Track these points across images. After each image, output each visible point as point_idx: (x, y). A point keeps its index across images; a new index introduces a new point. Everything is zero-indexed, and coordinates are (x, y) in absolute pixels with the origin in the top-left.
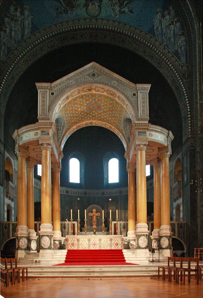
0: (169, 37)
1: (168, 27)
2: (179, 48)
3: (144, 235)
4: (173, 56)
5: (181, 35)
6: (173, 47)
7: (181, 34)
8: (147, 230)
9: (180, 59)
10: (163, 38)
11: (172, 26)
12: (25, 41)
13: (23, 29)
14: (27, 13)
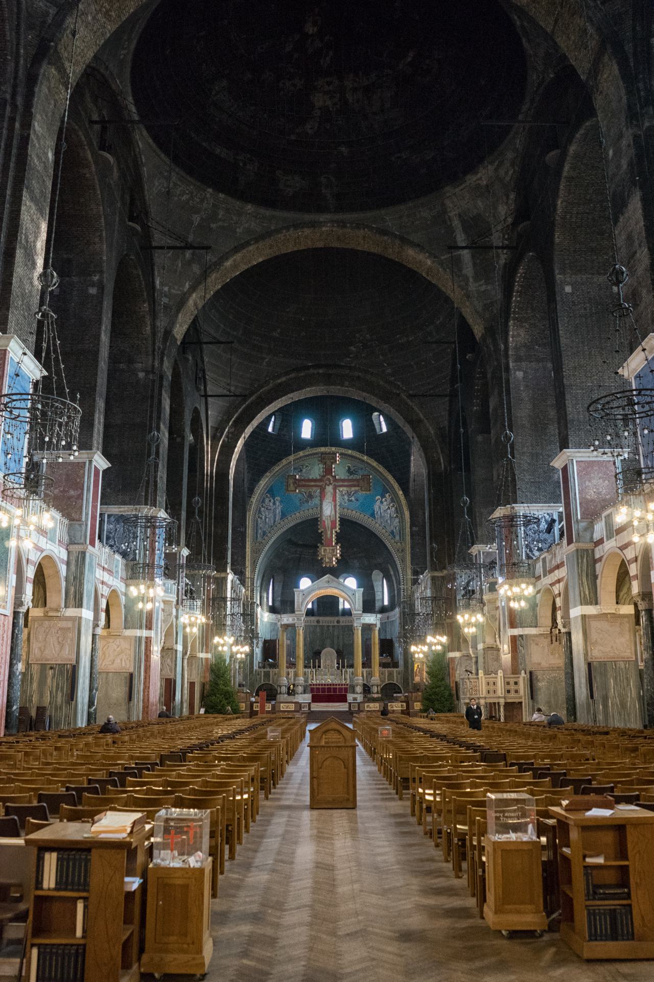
14: (277, 503)
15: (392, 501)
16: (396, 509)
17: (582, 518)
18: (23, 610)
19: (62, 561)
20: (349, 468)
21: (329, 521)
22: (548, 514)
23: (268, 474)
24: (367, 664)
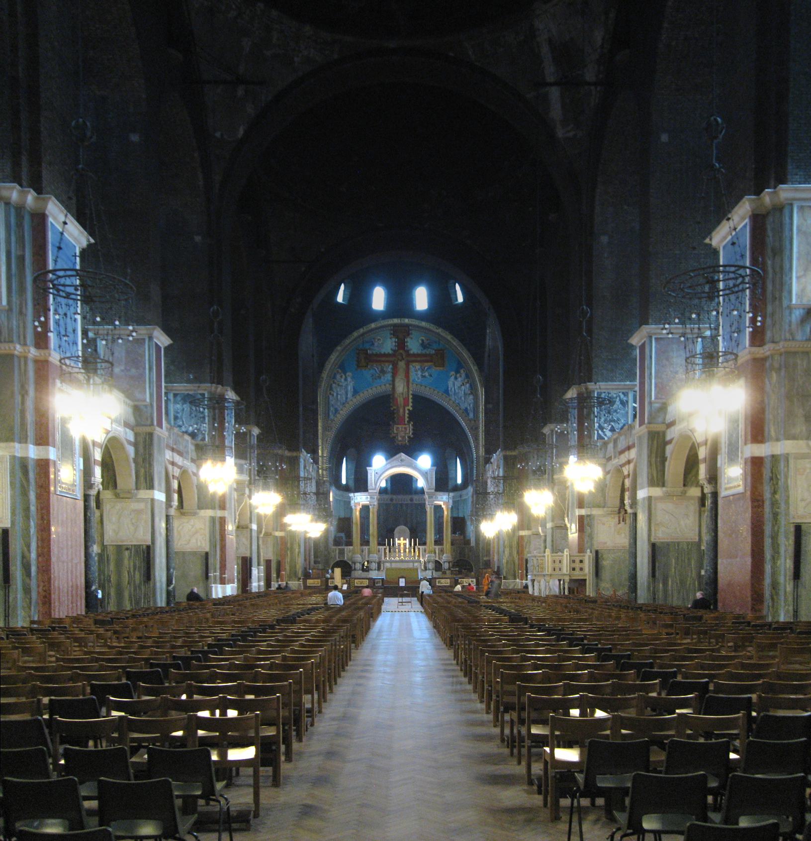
1: (459, 388)
11: (463, 387)
13: (347, 394)
14: (349, 379)
15: (467, 376)
16: (471, 386)
17: (656, 398)
18: (93, 492)
19: (129, 442)
20: (423, 341)
21: (402, 399)
22: (623, 393)
23: (339, 348)
24: (439, 542)
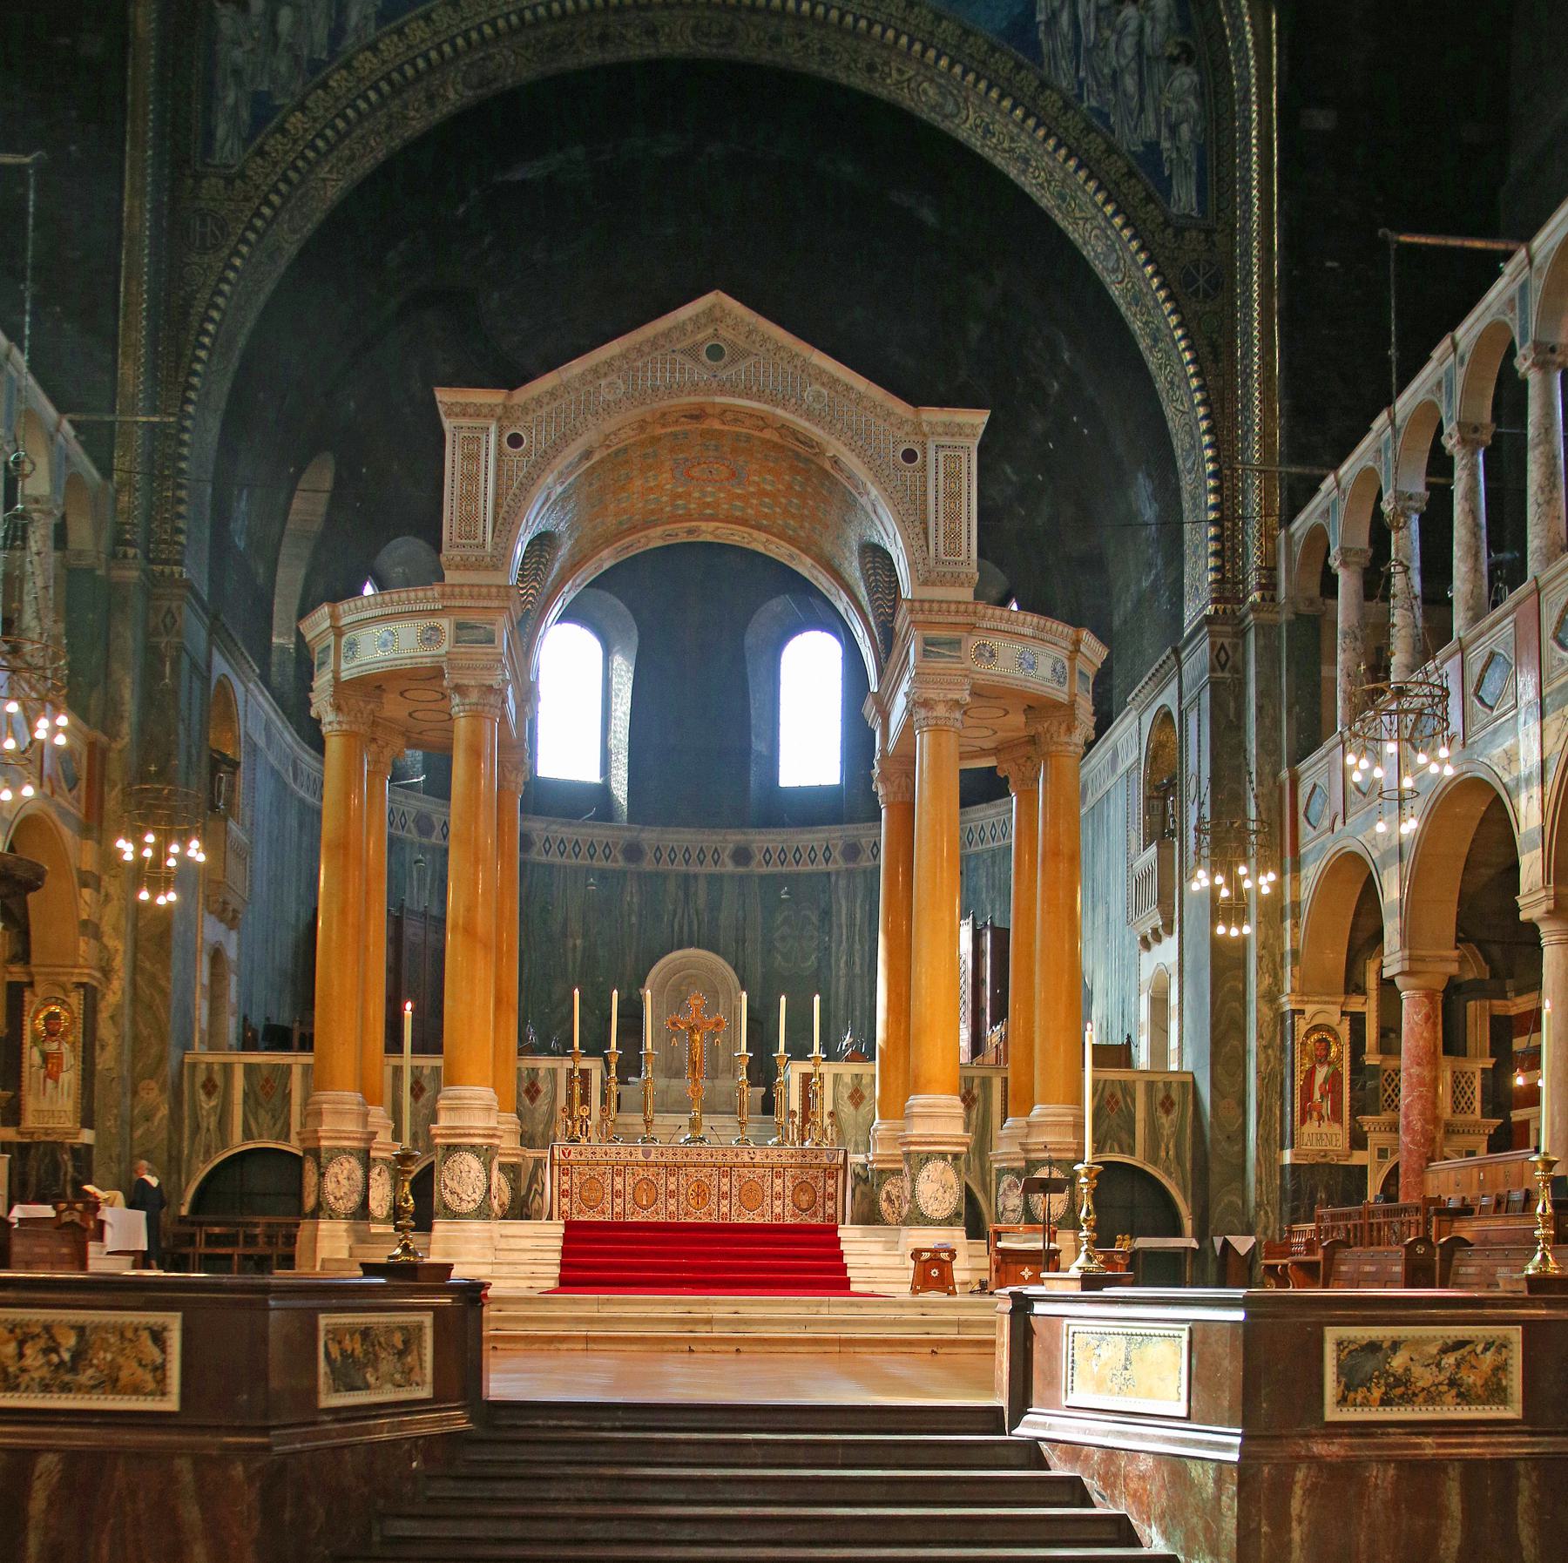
0: (1115, 72)
2: (1165, 132)
3: (943, 1156)
4: (1131, 174)
5: (1173, 60)
6: (1132, 124)
7: (1176, 52)
8: (960, 1132)
9: (1167, 193)
10: (1082, 74)
12: (348, 66)
